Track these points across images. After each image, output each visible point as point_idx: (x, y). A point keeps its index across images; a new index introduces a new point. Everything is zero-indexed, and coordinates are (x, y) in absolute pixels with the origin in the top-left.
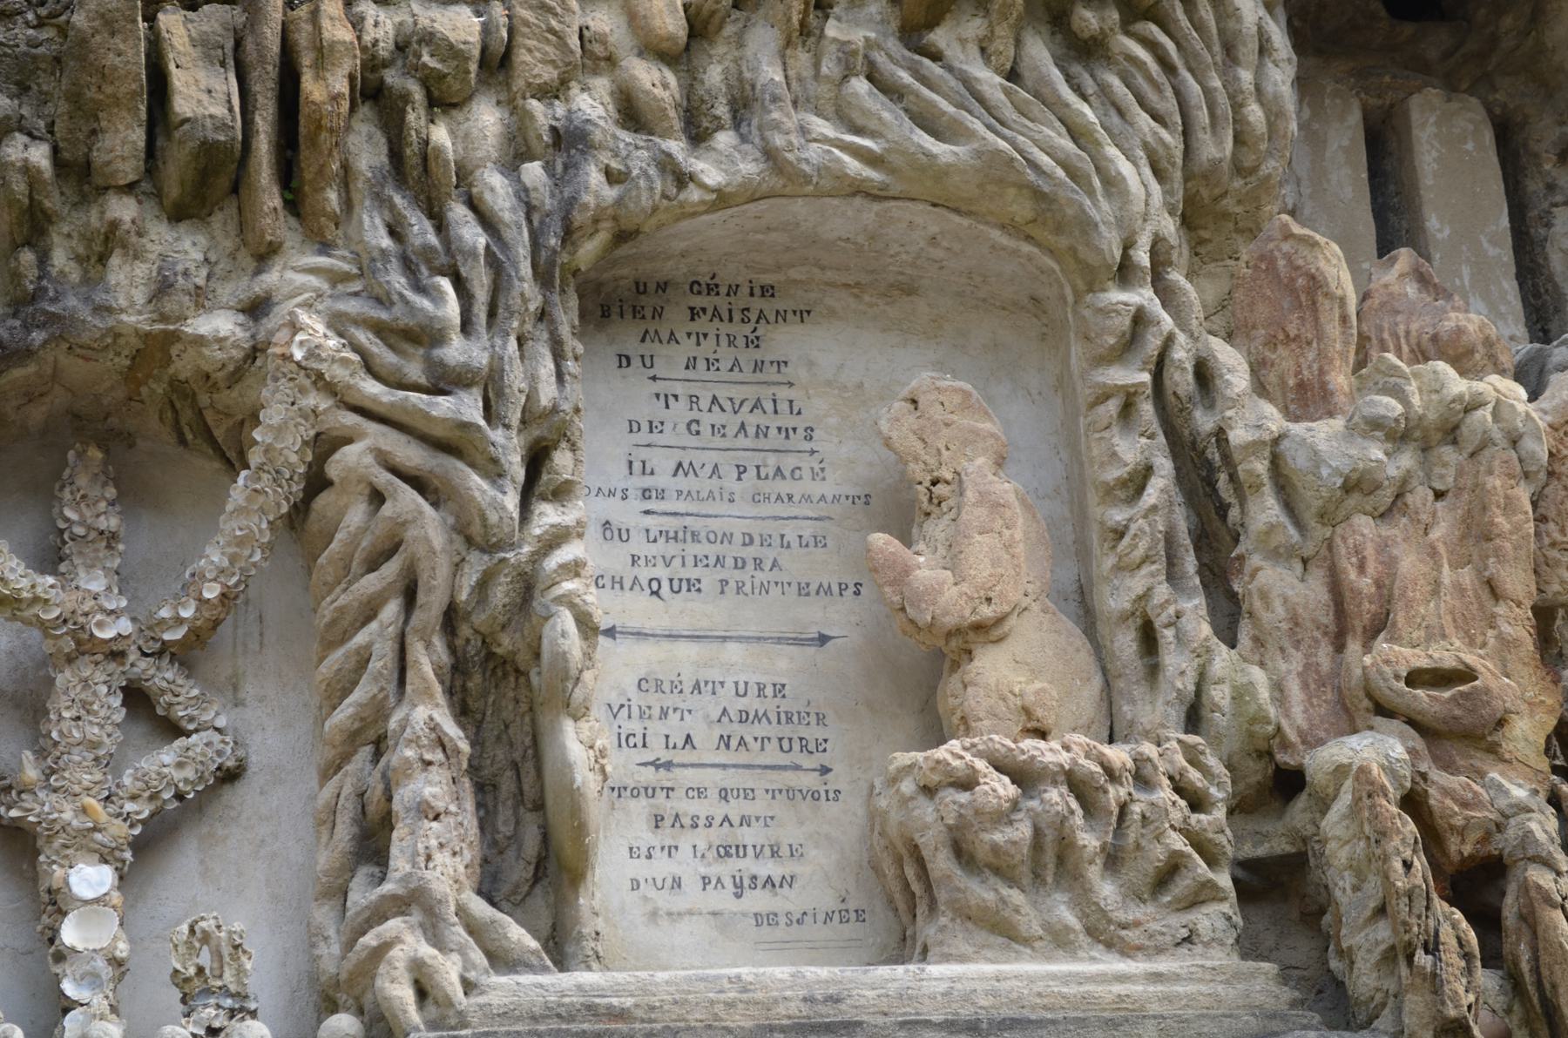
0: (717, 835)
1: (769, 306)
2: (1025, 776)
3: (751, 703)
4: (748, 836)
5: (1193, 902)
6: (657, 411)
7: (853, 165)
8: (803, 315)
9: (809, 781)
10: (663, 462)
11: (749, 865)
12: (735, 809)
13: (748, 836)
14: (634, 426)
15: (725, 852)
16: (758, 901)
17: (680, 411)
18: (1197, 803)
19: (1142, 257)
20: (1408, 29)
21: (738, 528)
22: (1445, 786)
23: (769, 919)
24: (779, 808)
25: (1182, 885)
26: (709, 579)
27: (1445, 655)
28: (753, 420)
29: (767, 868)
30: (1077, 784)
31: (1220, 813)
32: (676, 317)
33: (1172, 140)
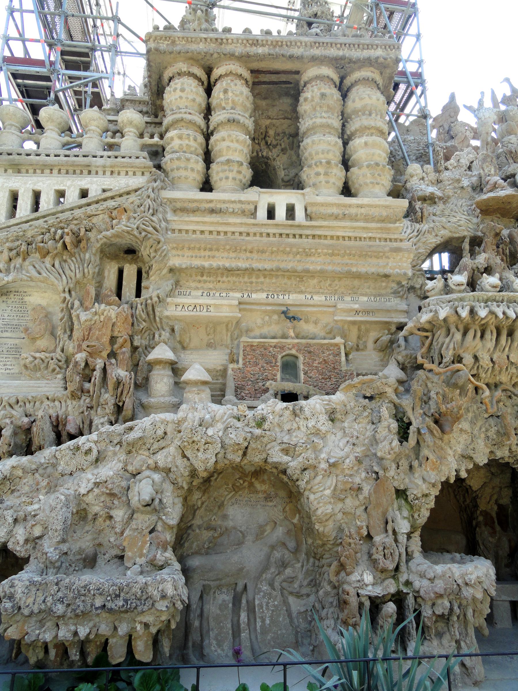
0: (4, 363)
1: (25, 294)
2: (35, 358)
3: (12, 346)
4: (8, 363)
5: (57, 374)
6: (7, 308)
7: (25, 278)
8: (30, 295)
9: (17, 356)
10: (6, 315)
11: (8, 367)
12: (7, 360)
13: (8, 363)
14: (3, 310)
15: (5, 365)
16: (8, 371)
17: (10, 308)
18: (60, 361)
19: (67, 290)
20: (126, 255)
21: (15, 323)
22: (90, 360)
23: (9, 374)
24: (13, 360)
25: (56, 372)
26: (9, 330)
27: (93, 344)
28: (20, 309)
29: (11, 367)
30: (42, 360)
31: (63, 362)
32: (12, 296)
33: (73, 274)
